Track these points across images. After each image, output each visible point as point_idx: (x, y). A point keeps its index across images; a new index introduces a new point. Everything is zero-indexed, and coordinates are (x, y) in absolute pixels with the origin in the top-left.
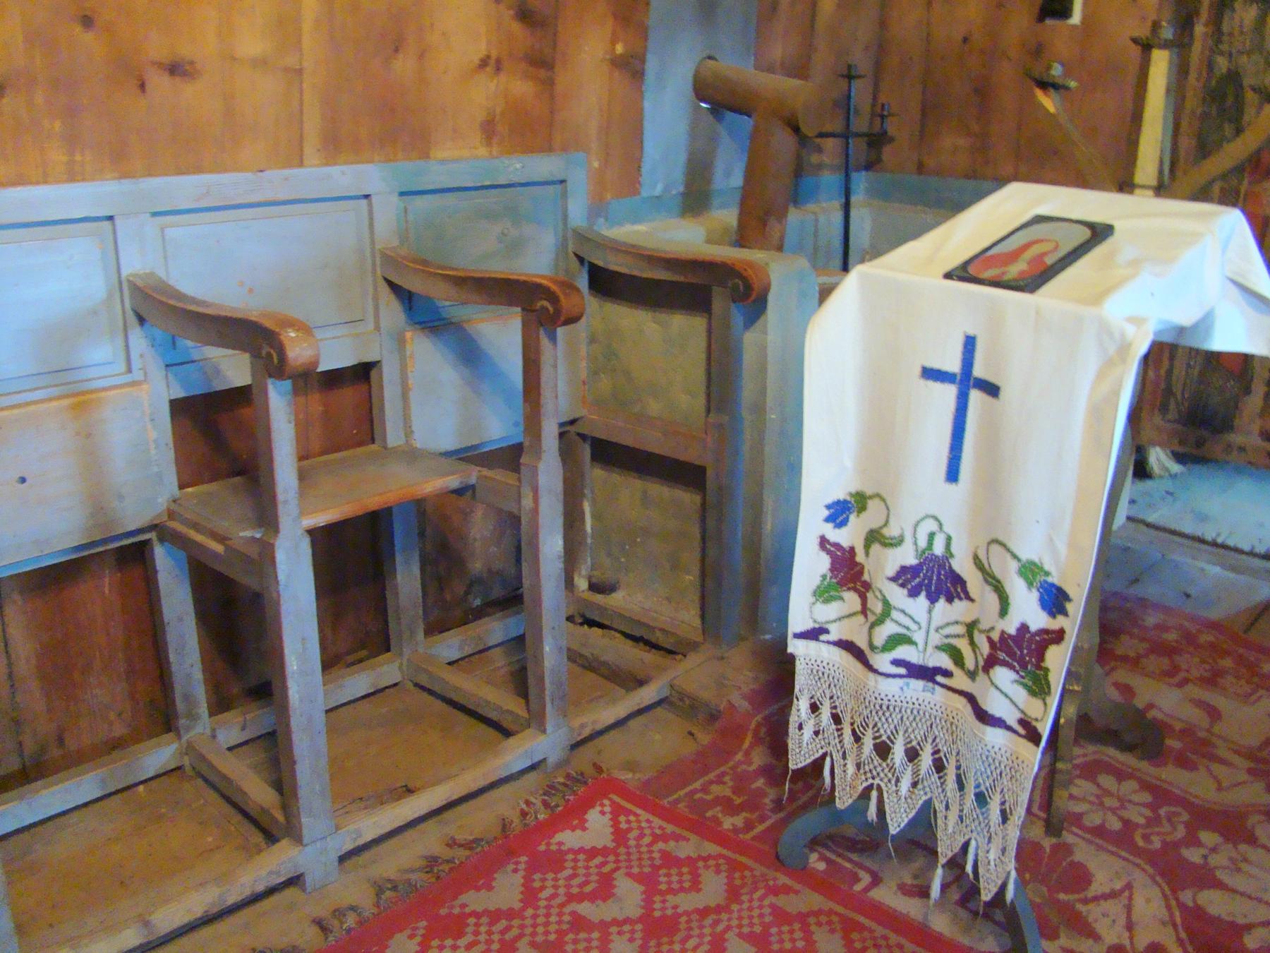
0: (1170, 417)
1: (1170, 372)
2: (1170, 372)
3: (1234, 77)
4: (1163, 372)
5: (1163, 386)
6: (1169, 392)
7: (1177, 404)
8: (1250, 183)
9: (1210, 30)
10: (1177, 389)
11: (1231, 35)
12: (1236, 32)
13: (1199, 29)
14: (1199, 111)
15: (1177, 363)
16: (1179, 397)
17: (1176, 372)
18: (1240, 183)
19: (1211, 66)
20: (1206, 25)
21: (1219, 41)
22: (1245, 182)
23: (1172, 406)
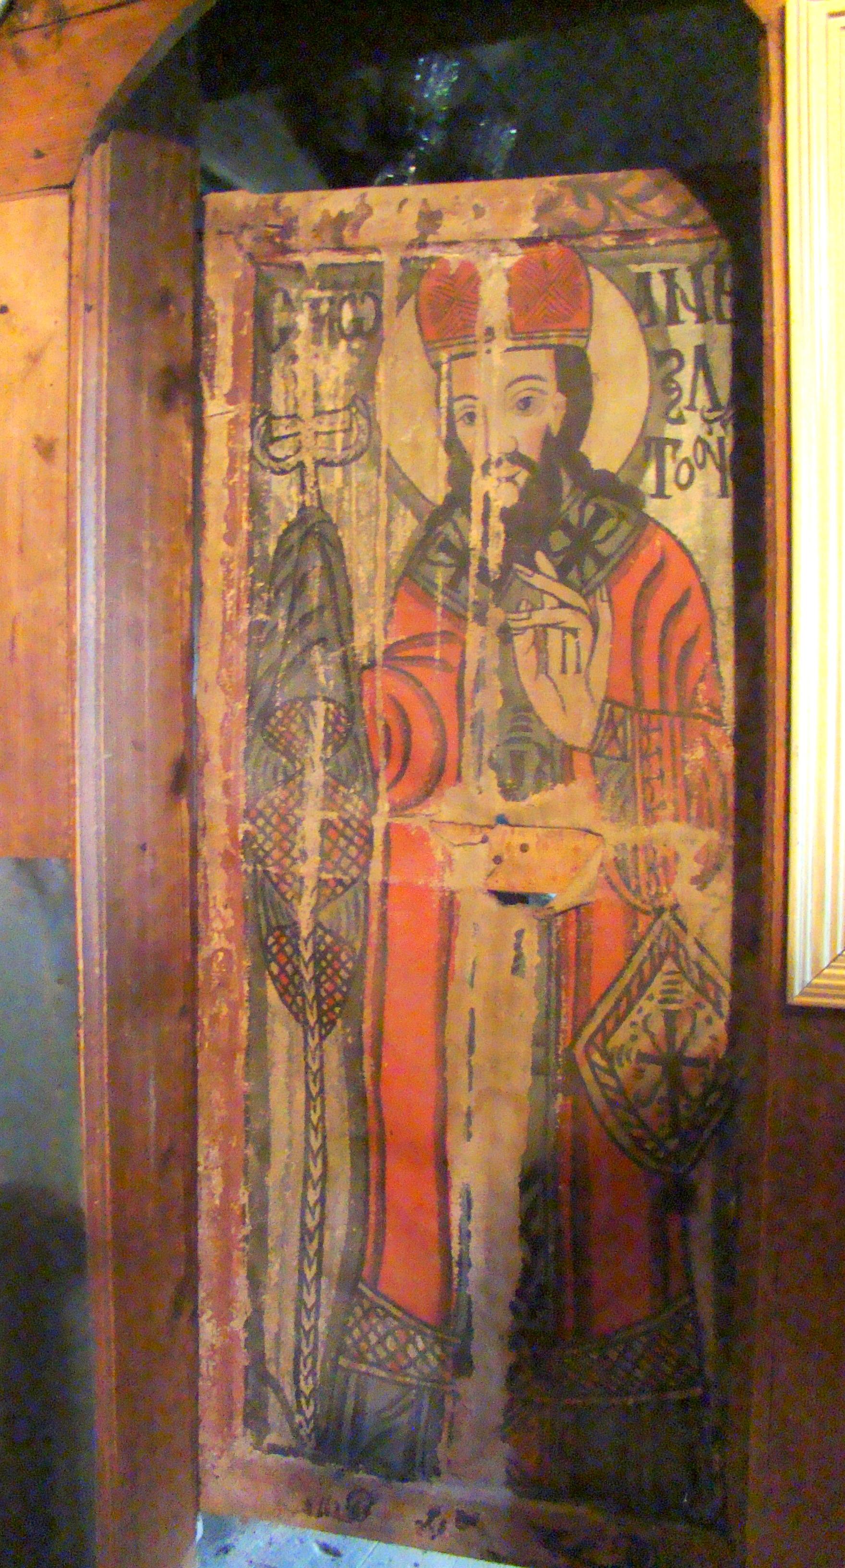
0: (272, 1438)
1: (254, 1325)
2: (254, 1325)
3: (315, 529)
4: (237, 1324)
5: (242, 1359)
6: (259, 1373)
7: (284, 1402)
8: (395, 810)
9: (244, 408)
10: (281, 1367)
11: (294, 417)
12: (306, 410)
13: (217, 409)
14: (244, 625)
15: (267, 1298)
16: (289, 1393)
17: (270, 1324)
18: (371, 809)
19: (257, 501)
20: (232, 398)
21: (269, 440)
22: (384, 806)
23: (274, 1413)
